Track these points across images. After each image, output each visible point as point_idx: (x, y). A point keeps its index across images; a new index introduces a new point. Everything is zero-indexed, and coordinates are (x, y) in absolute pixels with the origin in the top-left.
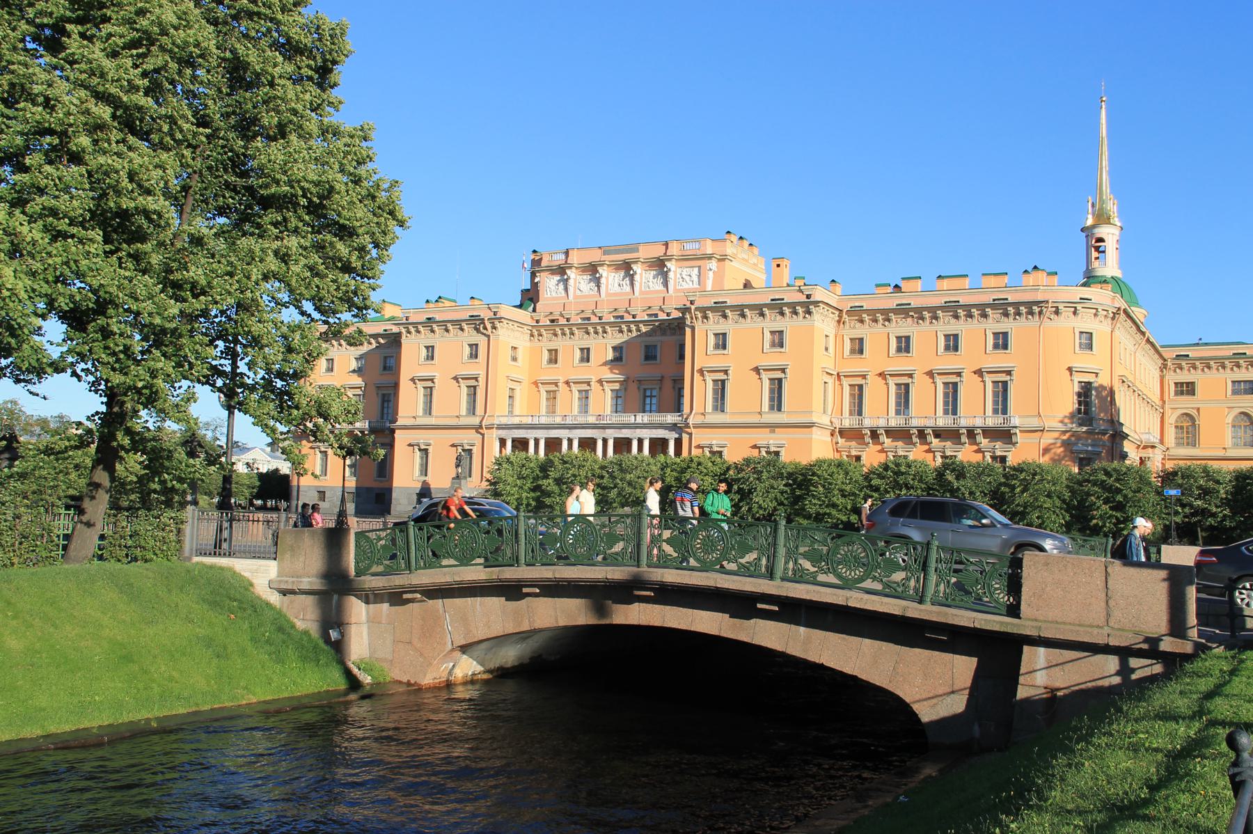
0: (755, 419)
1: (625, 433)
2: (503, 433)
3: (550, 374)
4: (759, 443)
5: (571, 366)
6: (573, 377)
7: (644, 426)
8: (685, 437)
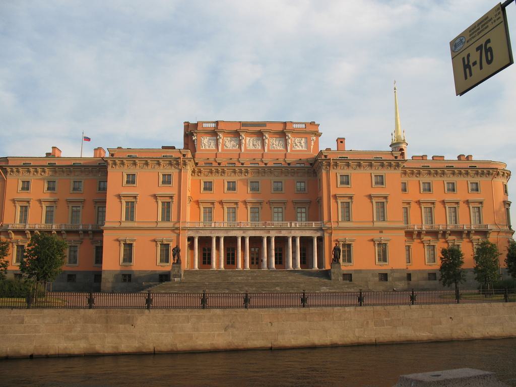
0: (370, 225)
1: (283, 234)
2: (191, 234)
3: (207, 196)
4: (375, 239)
5: (220, 192)
6: (224, 199)
7: (297, 229)
8: (326, 236)
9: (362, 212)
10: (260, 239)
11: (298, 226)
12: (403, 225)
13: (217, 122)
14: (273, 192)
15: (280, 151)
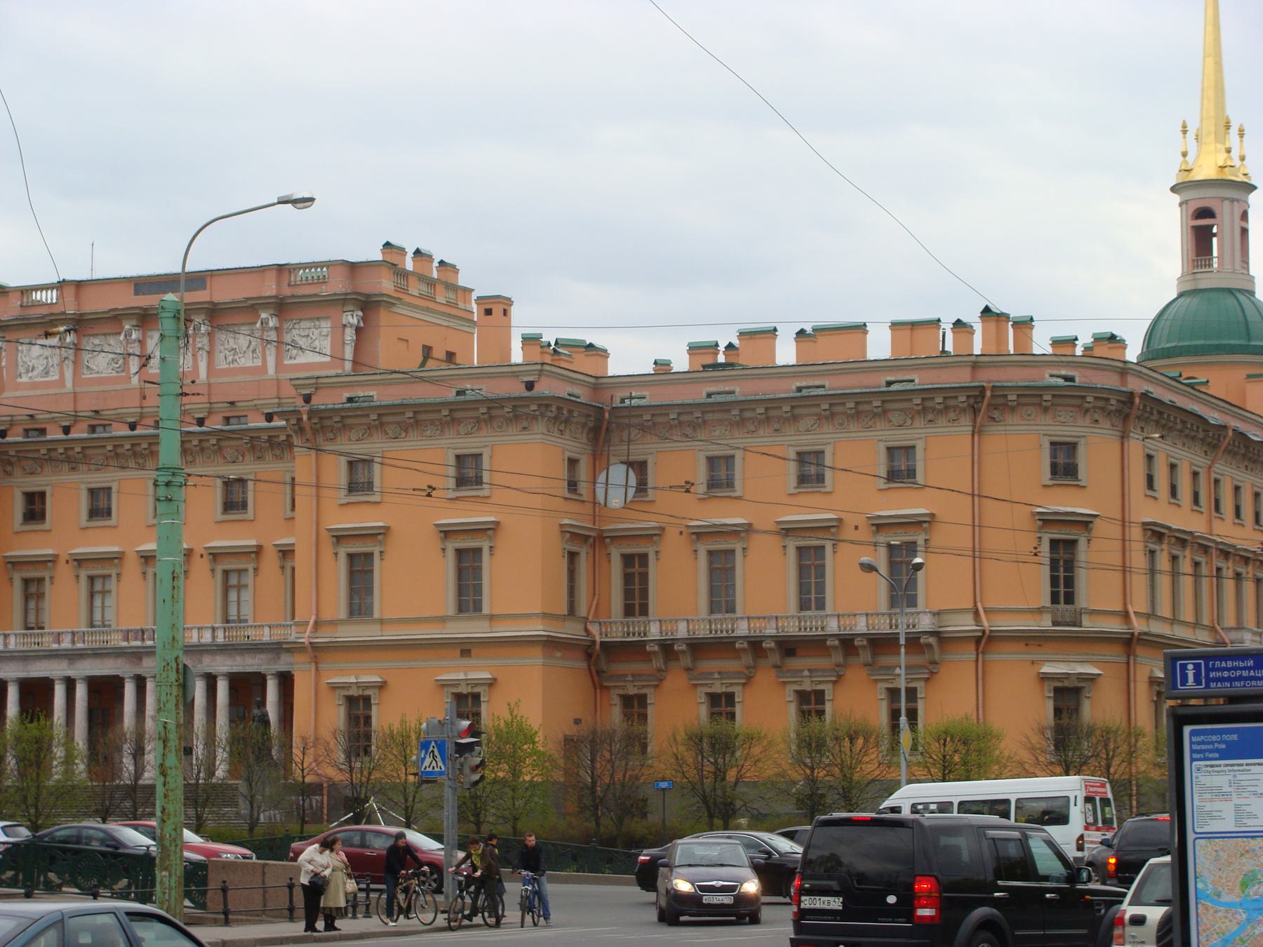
9: (414, 587)
10: (258, 680)
11: (220, 639)
12: (536, 629)
13: (61, 285)
14: (220, 517)
15: (245, 370)
